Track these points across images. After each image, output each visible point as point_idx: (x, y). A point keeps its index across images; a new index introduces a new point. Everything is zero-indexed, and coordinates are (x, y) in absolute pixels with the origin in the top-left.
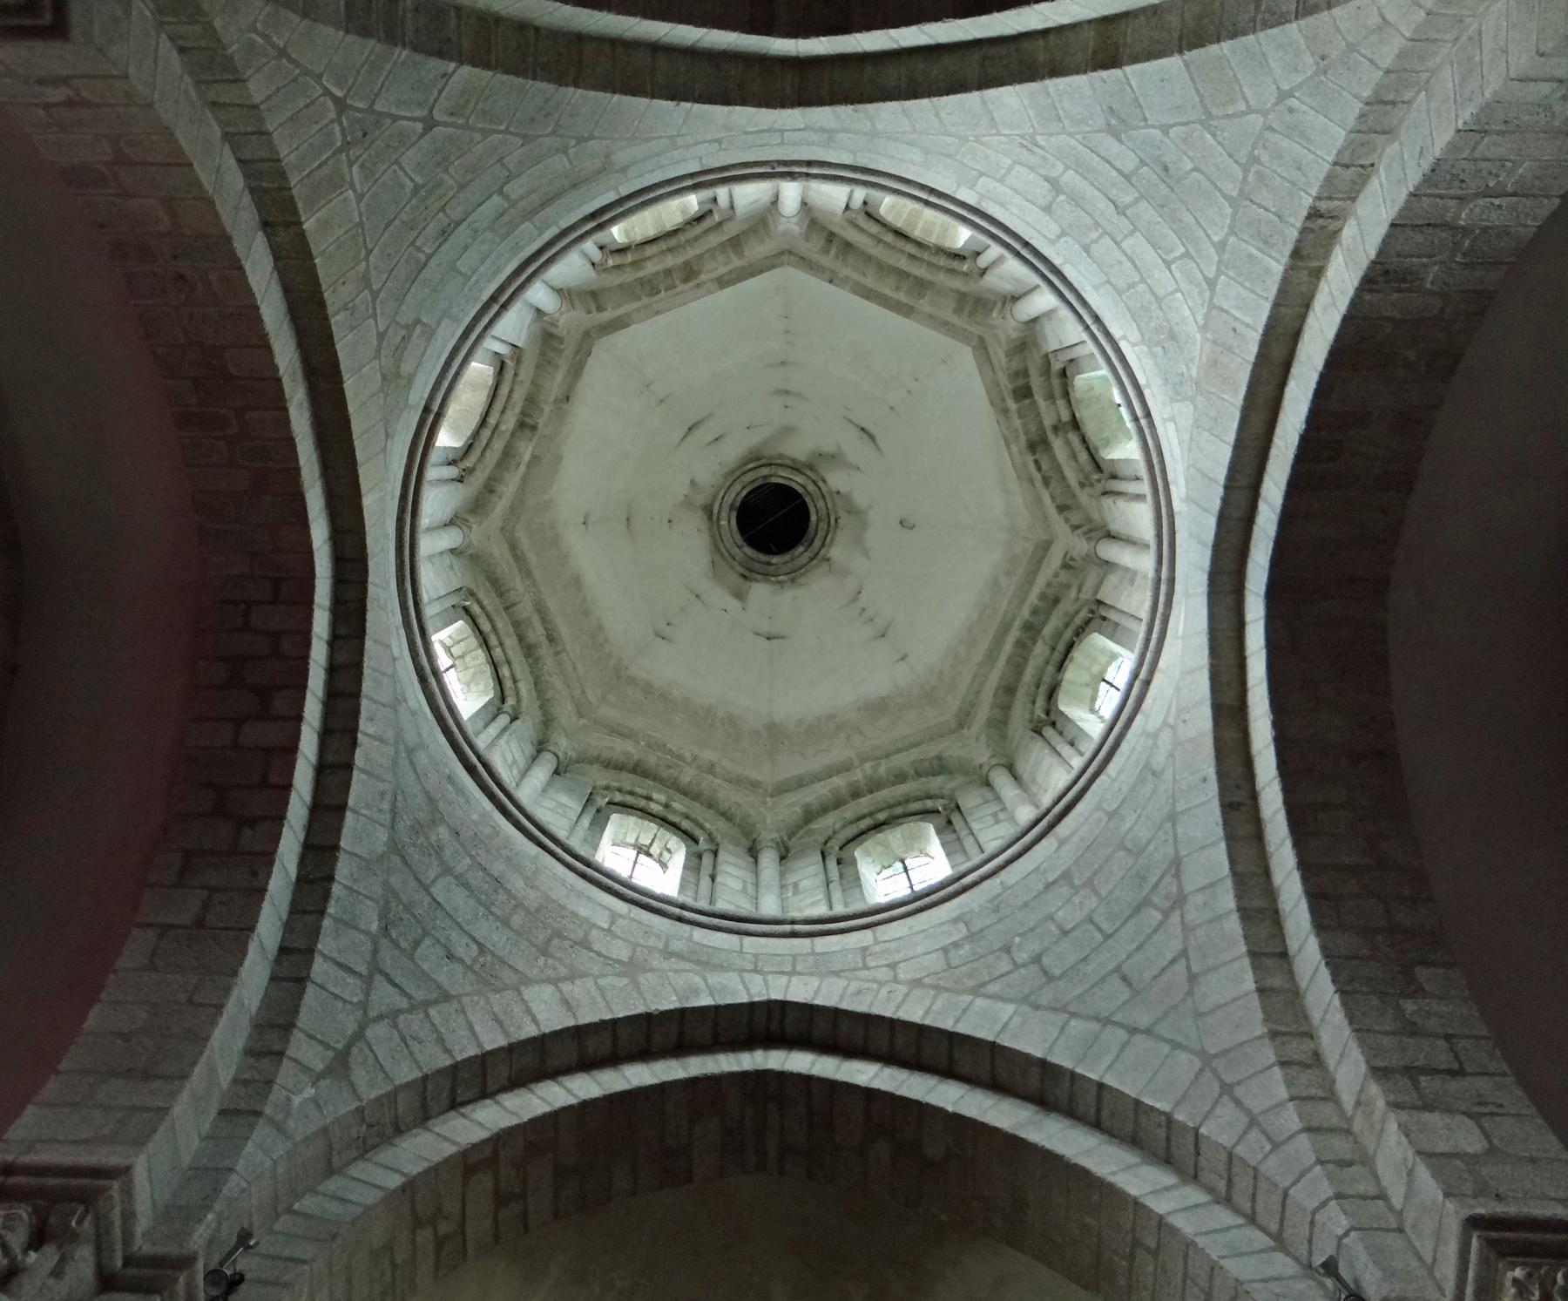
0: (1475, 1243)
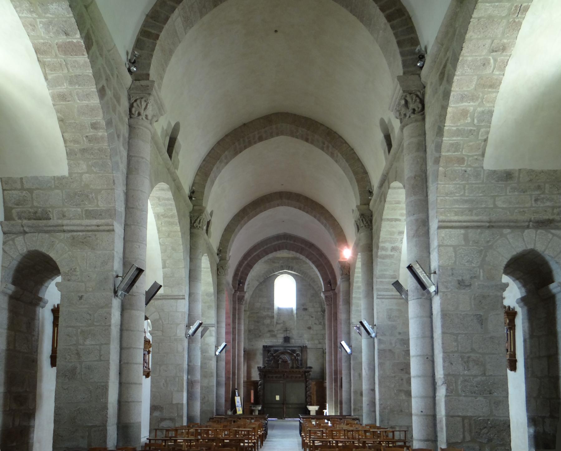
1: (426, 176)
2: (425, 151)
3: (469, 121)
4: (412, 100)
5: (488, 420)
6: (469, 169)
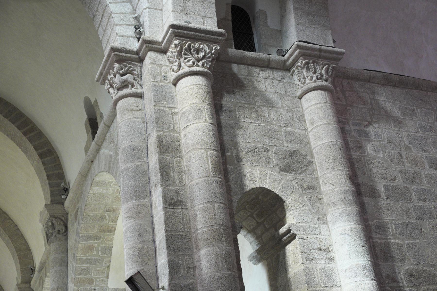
0: (170, 31)
1: (67, 287)
2: (67, 266)
3: (95, 253)
6: (98, 288)
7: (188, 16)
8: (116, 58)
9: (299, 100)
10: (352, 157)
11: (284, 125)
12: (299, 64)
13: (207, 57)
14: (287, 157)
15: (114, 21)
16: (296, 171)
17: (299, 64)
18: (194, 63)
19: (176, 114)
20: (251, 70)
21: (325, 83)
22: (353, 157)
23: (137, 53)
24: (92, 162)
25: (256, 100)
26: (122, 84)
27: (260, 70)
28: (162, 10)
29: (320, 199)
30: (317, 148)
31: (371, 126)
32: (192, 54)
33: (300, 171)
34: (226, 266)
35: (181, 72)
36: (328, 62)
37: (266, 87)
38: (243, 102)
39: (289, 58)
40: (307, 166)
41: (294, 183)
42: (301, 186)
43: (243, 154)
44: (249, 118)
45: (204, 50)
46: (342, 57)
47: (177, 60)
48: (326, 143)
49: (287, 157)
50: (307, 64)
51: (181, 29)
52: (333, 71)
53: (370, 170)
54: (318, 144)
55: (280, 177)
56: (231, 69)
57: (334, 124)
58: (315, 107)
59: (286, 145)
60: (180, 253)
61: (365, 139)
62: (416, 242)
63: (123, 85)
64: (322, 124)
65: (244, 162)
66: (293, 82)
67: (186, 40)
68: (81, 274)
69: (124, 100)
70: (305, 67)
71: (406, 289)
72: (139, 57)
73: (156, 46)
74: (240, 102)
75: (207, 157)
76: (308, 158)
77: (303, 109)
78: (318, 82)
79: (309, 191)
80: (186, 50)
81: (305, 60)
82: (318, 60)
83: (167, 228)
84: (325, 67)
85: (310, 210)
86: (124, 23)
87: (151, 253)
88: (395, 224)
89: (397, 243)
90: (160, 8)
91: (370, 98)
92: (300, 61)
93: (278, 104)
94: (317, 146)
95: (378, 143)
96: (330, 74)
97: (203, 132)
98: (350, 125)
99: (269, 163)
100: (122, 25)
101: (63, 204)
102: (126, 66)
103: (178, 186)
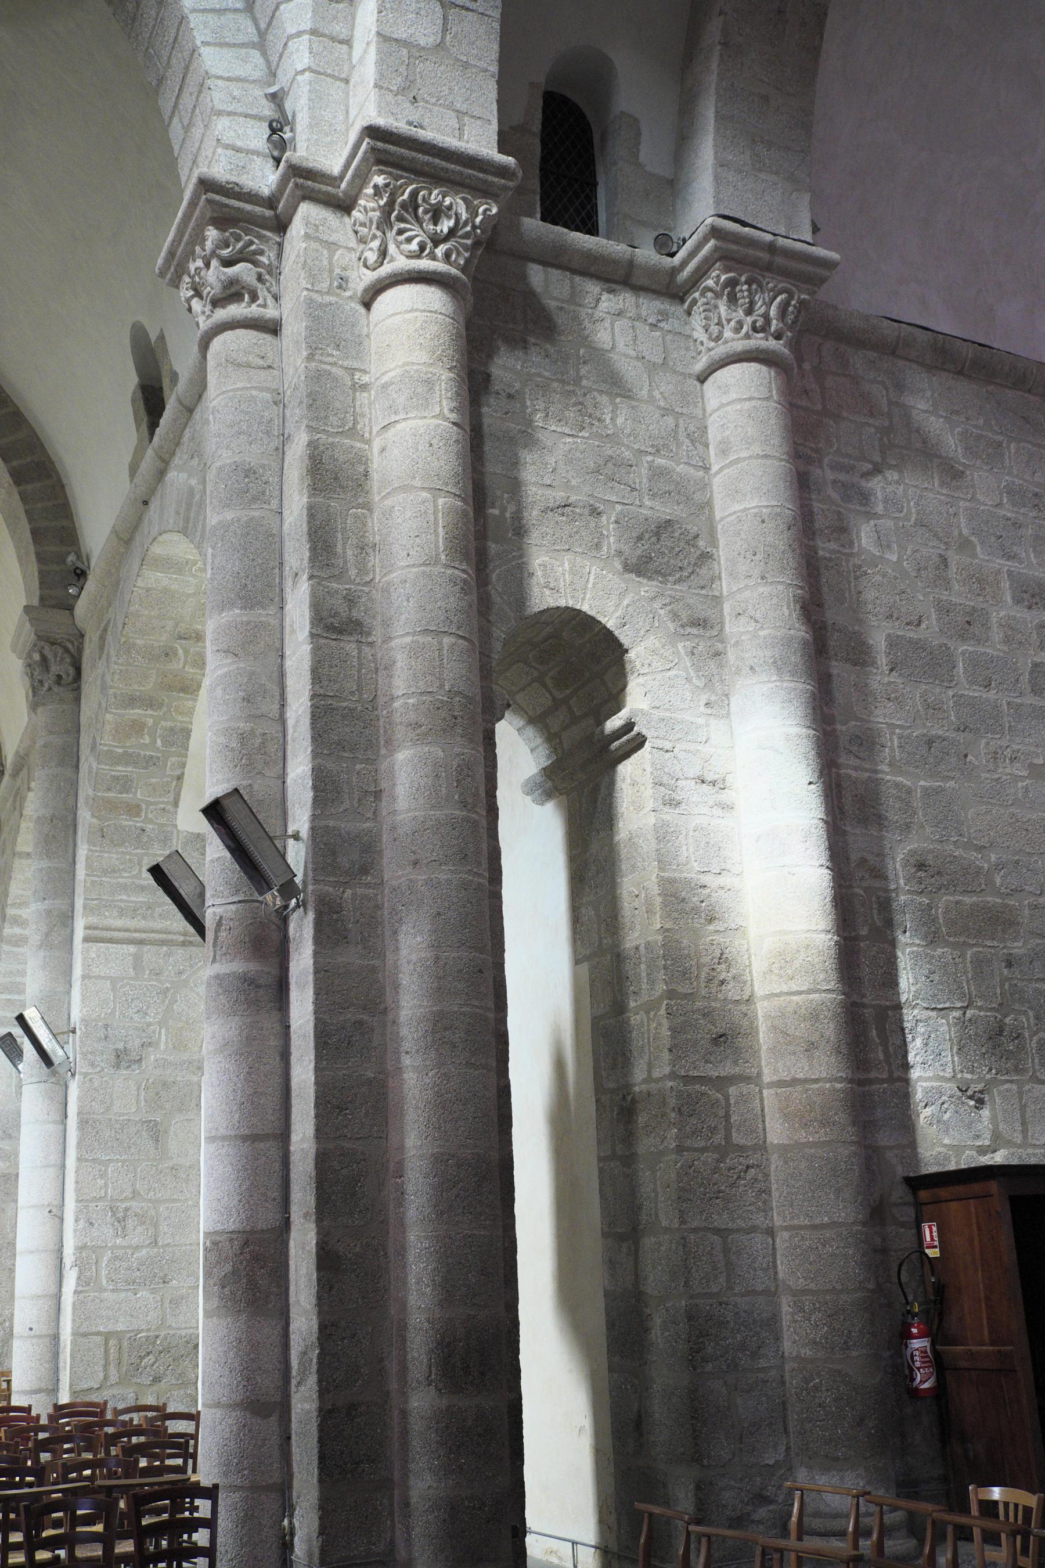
1: (75, 819)
2: (77, 767)
3: (147, 742)
4: (56, 657)
5: (157, 1337)
6: (151, 827)
7: (417, 107)
8: (214, 211)
9: (698, 384)
10: (816, 553)
11: (650, 450)
12: (710, 283)
13: (460, 233)
14: (647, 536)
15: (212, 101)
16: (664, 576)
17: (710, 283)
18: (422, 247)
19: (364, 387)
20: (579, 288)
21: (772, 344)
22: (821, 553)
23: (271, 202)
24: (146, 503)
25: (583, 372)
26: (225, 288)
27: (603, 290)
28: (347, 81)
29: (717, 654)
30: (729, 519)
31: (880, 477)
32: (419, 221)
33: (678, 576)
34: (456, 797)
35: (386, 269)
36: (789, 286)
37: (613, 340)
38: (547, 374)
39: (684, 263)
40: (695, 564)
41: (657, 605)
42: (675, 616)
43: (532, 515)
44: (560, 420)
45: (453, 212)
46: (828, 274)
47: (379, 233)
48: (752, 508)
49: (647, 536)
50: (732, 283)
51: (393, 144)
52: (799, 312)
53: (860, 592)
54: (733, 509)
55: (622, 585)
56: (524, 277)
57: (782, 460)
58: (738, 407)
59: (648, 503)
60: (346, 755)
61: (858, 508)
62: (947, 785)
63: (229, 292)
64: (750, 457)
65: (534, 538)
66: (688, 332)
67: (406, 178)
68: (109, 789)
69: (228, 335)
70: (726, 292)
71: (902, 898)
72: (277, 216)
73: (324, 188)
74: (539, 375)
75: (435, 513)
76: (701, 543)
77: (704, 410)
78: (756, 338)
79: (694, 631)
80: (404, 206)
81: (727, 273)
82: (764, 277)
83: (317, 687)
84: (778, 299)
85: (688, 679)
86: (240, 110)
87: (272, 748)
88: (900, 737)
89: (897, 785)
90: (343, 76)
91: (888, 399)
92: (714, 274)
93: (641, 390)
94: (730, 515)
95: (890, 523)
96: (790, 318)
97: (431, 445)
98: (825, 467)
99: (598, 546)
100: (235, 114)
101: (71, 609)
102: (238, 239)
103: (352, 582)
